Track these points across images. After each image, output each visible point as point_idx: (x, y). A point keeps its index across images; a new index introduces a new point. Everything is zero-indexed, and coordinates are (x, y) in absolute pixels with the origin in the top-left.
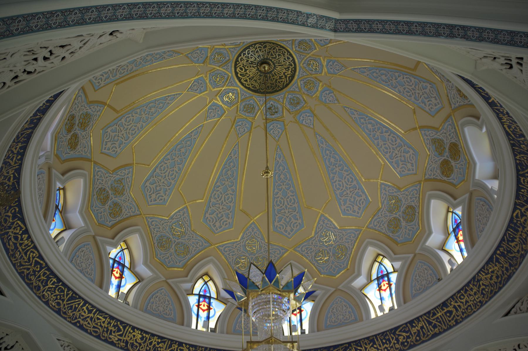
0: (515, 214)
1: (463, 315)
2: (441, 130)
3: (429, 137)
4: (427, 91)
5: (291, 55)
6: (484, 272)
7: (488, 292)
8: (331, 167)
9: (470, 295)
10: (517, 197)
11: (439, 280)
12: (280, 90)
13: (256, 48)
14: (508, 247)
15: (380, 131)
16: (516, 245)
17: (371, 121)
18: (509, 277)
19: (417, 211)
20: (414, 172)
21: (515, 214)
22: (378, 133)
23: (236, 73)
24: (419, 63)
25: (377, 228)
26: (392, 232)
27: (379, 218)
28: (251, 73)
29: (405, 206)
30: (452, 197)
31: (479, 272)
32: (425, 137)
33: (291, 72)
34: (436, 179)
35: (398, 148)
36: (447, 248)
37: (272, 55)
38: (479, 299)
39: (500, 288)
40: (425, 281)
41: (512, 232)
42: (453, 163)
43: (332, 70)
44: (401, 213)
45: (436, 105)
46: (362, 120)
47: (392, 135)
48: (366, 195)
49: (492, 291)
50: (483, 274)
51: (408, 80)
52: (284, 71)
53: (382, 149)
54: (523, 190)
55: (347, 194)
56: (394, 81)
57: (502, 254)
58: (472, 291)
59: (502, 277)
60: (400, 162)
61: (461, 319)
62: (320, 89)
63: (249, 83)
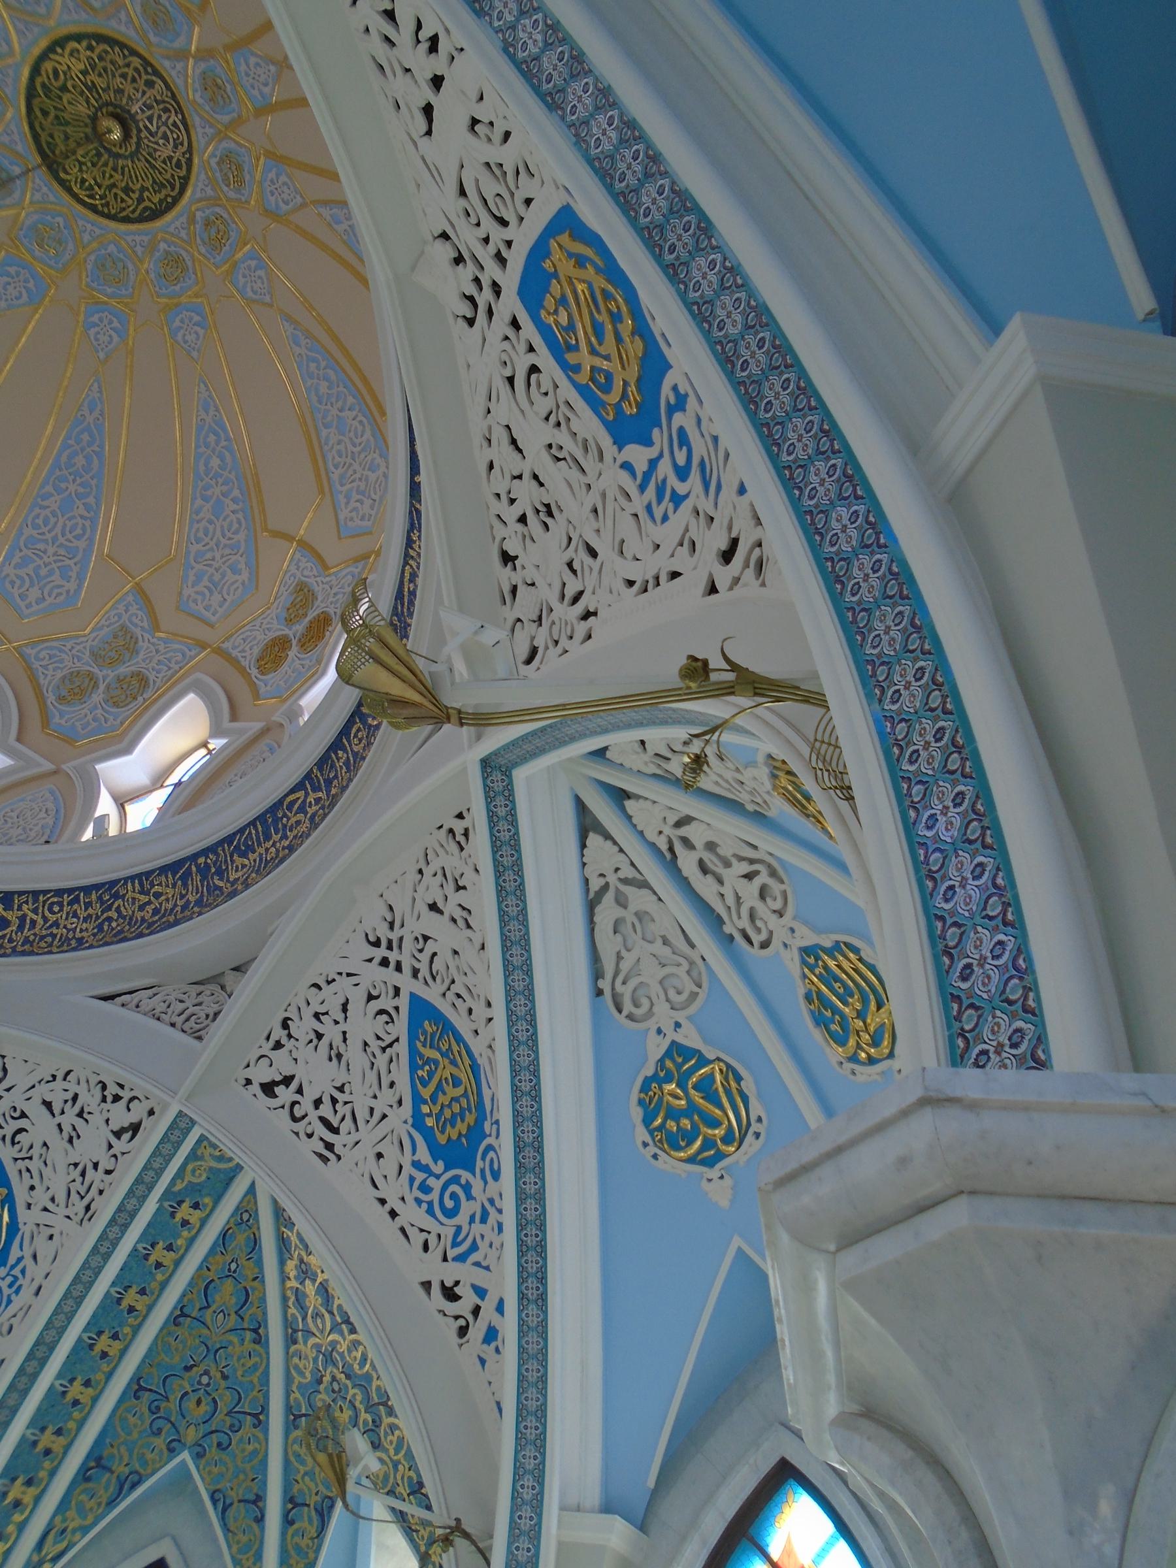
0: (292, 797)
1: (23, 945)
2: (329, 575)
3: (298, 574)
4: (372, 477)
5: (190, 162)
6: (141, 884)
7: (113, 929)
8: (65, 472)
9: (75, 915)
10: (324, 761)
11: (47, 842)
12: (102, 214)
13: (128, 65)
14: (226, 861)
15: (225, 488)
16: (244, 866)
17: (227, 454)
18: (177, 923)
19: (145, 696)
20: (213, 619)
21: (289, 799)
22: (217, 491)
23: (36, 71)
24: (303, 102)
25: (36, 665)
26: (61, 699)
27: (61, 651)
28: (69, 108)
29: (133, 668)
30: (228, 711)
31: (132, 878)
32: (293, 568)
33: (161, 201)
34: (239, 662)
35: (227, 551)
36: (129, 808)
37: (150, 119)
38: (85, 934)
39: (141, 935)
40: (20, 831)
41: (257, 831)
42: (293, 652)
43: (242, 280)
44: (111, 674)
45: (362, 519)
46: (212, 438)
47: (240, 515)
48: (80, 586)
49: (121, 931)
50: (137, 885)
51: (360, 428)
52: (148, 184)
53: (196, 526)
54: (340, 753)
55: (45, 552)
56: (334, 412)
57: (204, 871)
58: (86, 909)
59: (164, 916)
60: (206, 578)
61: (9, 951)
62: (184, 300)
63: (47, 123)
